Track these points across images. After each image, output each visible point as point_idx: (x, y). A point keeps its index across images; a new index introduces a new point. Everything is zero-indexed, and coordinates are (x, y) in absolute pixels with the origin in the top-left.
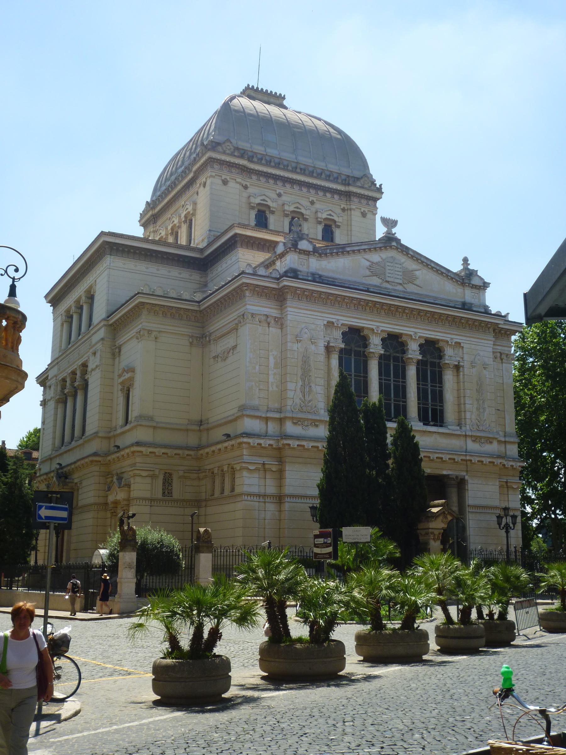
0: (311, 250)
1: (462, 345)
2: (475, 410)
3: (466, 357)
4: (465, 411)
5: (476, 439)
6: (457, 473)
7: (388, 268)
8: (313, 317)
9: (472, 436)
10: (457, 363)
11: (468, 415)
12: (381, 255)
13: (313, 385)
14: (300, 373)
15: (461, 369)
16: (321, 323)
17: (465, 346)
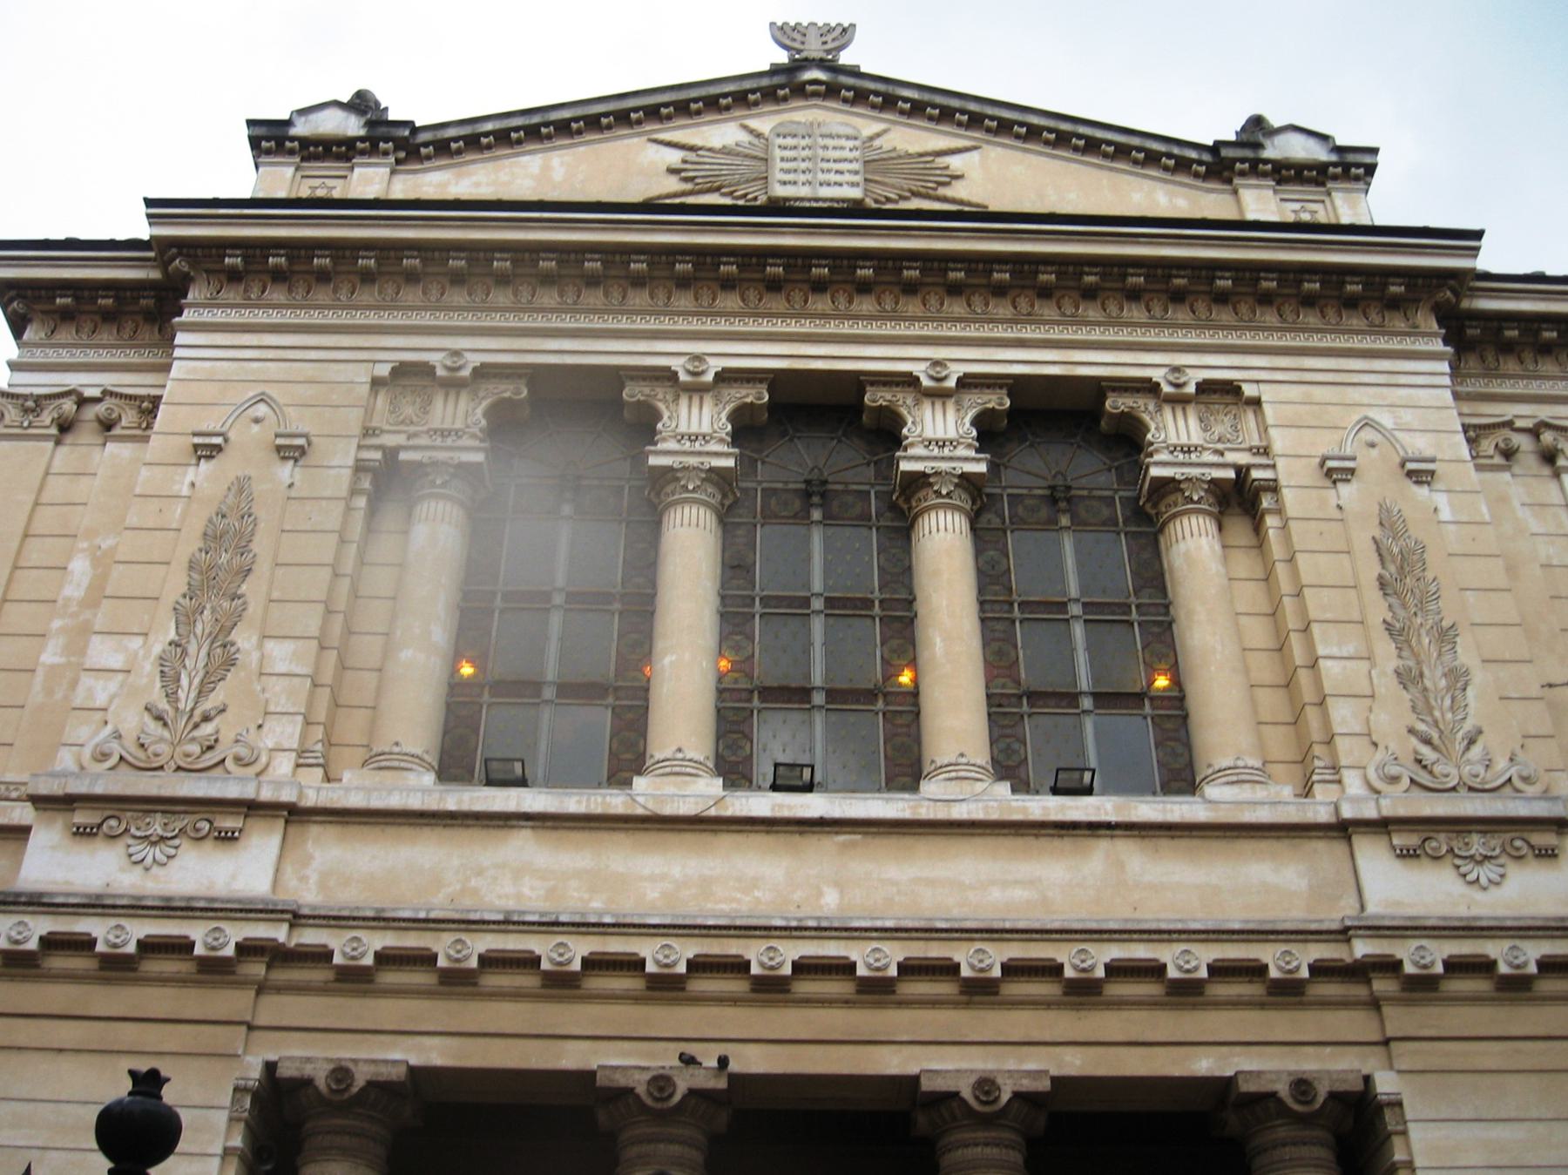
0: (362, 132)
1: (1249, 390)
2: (1386, 683)
3: (1280, 441)
4: (1322, 703)
5: (1418, 836)
6: (1308, 1063)
7: (778, 153)
8: (313, 355)
9: (1383, 826)
10: (1231, 474)
11: (1343, 715)
12: (753, 123)
13: (244, 639)
14: (175, 584)
15: (1266, 502)
16: (362, 375)
17: (1267, 393)
